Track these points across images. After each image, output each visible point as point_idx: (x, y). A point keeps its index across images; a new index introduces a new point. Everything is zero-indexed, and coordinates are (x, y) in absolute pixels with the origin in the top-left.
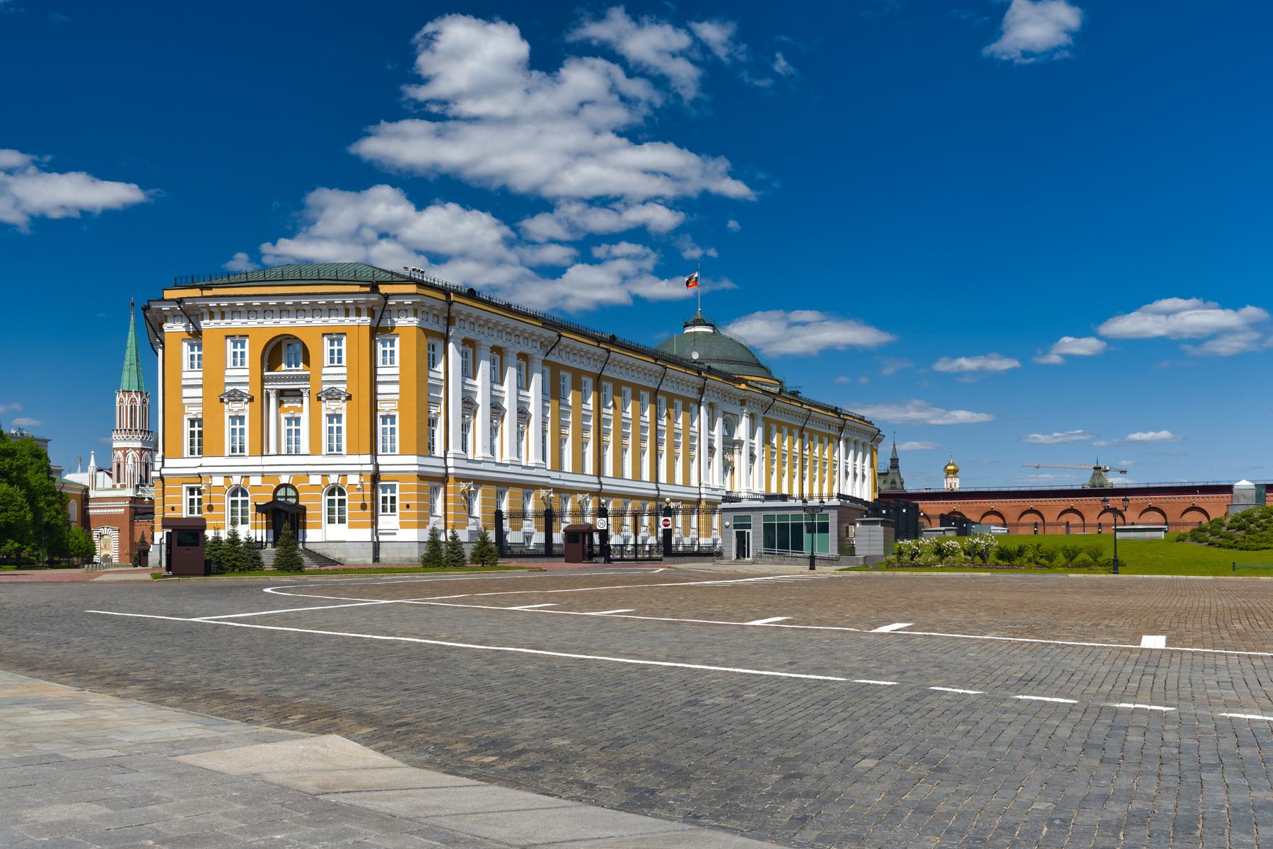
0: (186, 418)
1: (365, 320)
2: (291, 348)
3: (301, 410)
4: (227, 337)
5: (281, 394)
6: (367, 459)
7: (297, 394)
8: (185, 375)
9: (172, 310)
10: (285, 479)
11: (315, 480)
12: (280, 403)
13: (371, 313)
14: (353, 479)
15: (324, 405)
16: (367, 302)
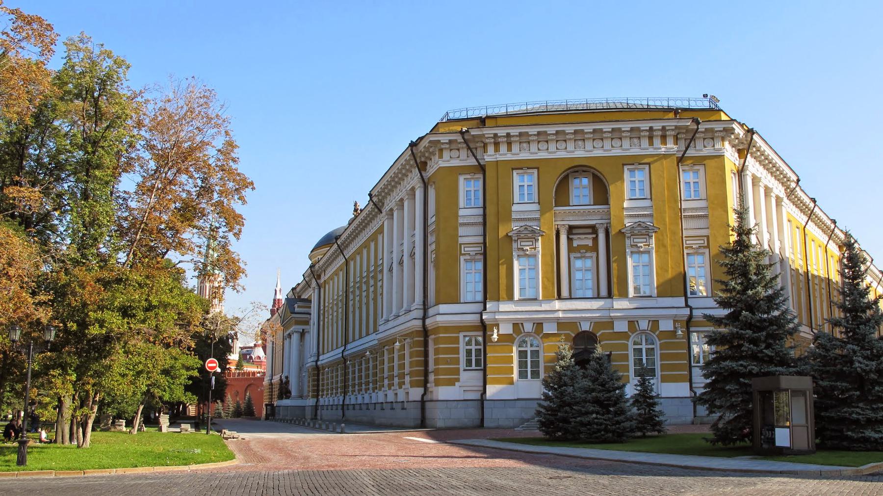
0: (462, 258)
1: (671, 147)
2: (577, 181)
3: (595, 248)
4: (513, 169)
5: (571, 229)
6: (681, 301)
7: (594, 229)
8: (461, 212)
9: (450, 142)
10: (586, 327)
11: (621, 327)
12: (570, 240)
13: (676, 140)
14: (666, 326)
15: (628, 242)
16: (676, 127)
